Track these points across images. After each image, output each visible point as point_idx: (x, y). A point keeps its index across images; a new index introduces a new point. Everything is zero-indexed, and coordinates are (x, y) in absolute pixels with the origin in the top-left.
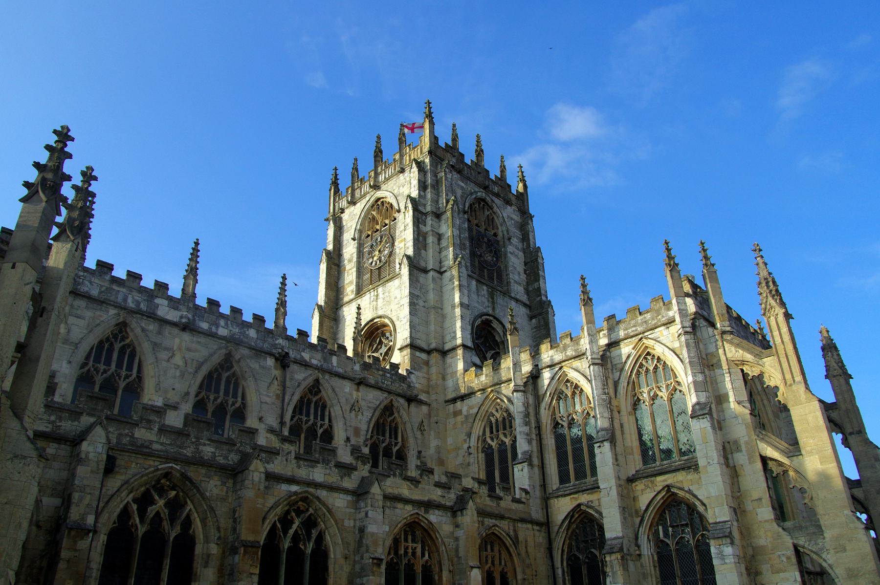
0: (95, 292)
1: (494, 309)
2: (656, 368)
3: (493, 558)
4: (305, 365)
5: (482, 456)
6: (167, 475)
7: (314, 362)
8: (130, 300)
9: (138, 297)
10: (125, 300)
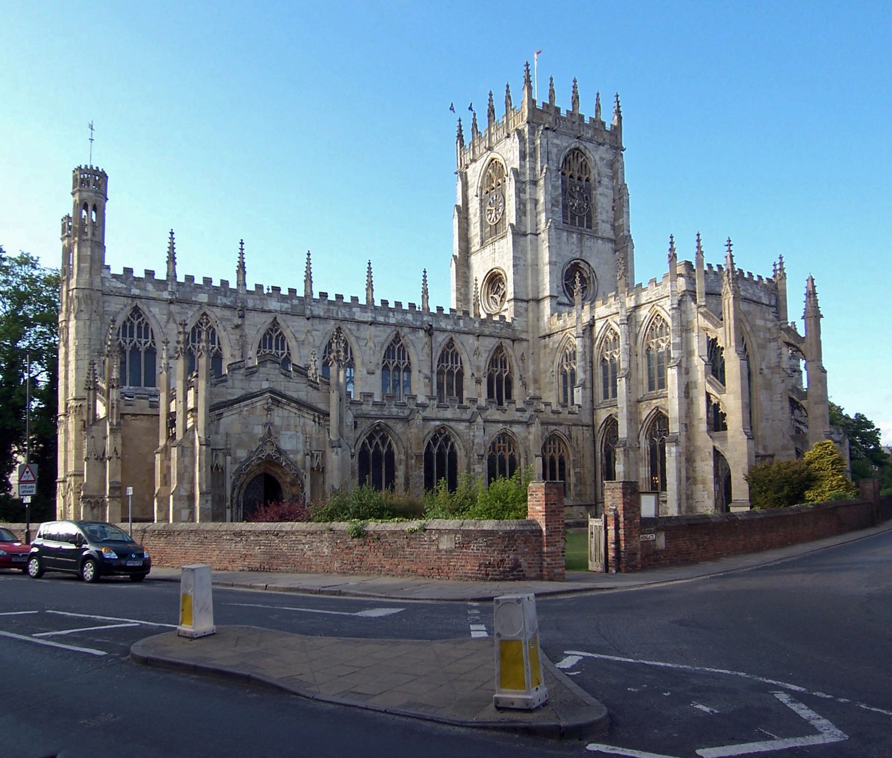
0: (322, 314)
4: (444, 331)
5: (561, 377)
6: (379, 425)
7: (449, 327)
10: (337, 314)
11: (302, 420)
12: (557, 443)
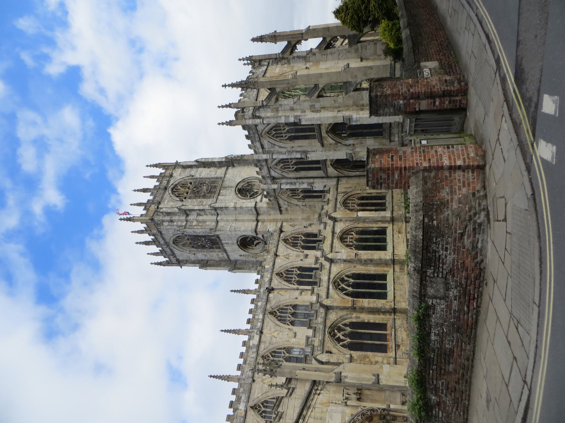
1: (232, 187)
2: (275, 130)
3: (352, 203)
4: (271, 280)
5: (306, 200)
6: (330, 333)
7: (269, 276)
8: (253, 356)
9: (250, 352)
10: (253, 358)
11: (317, 406)
12: (350, 202)
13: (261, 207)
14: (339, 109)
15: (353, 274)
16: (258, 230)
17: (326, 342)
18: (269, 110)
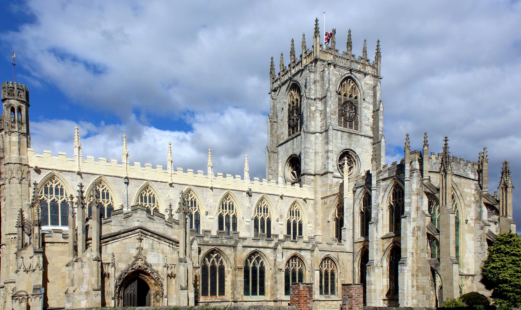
13: (328, 178)
14: (415, 254)
15: (264, 268)
16: (305, 176)
17: (207, 247)
18: (419, 186)
